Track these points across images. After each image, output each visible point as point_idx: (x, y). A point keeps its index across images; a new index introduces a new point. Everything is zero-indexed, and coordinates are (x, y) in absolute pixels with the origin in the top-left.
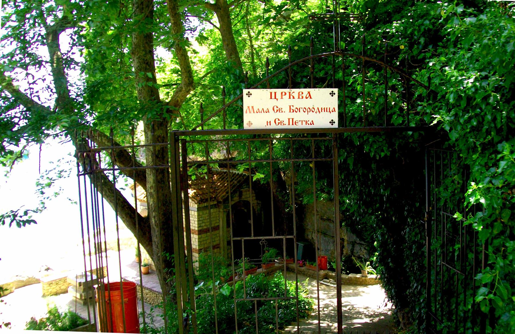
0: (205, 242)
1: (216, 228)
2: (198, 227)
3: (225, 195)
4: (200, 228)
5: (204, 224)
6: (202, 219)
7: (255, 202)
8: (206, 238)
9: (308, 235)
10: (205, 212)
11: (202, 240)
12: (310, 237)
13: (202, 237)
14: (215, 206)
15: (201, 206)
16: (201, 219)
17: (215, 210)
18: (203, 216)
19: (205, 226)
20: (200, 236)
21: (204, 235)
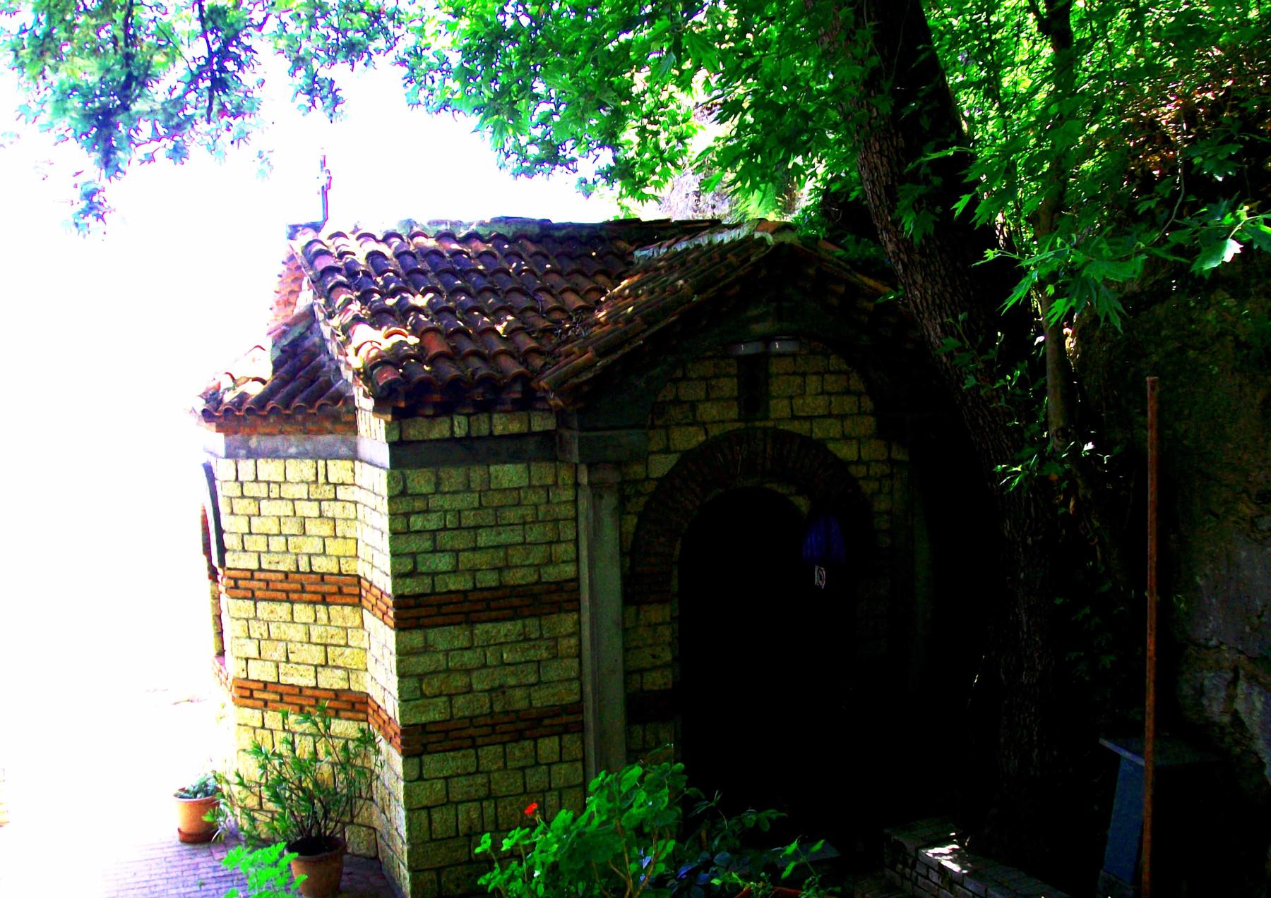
0: (459, 681)
1: (554, 598)
2: (397, 576)
3: (589, 366)
4: (411, 586)
5: (443, 562)
6: (433, 522)
7: (874, 450)
8: (469, 658)
9: (1200, 691)
10: (454, 477)
11: (422, 664)
12: (1215, 709)
13: (427, 649)
14: (547, 447)
15: (417, 430)
16: (417, 522)
17: (544, 472)
18: (435, 502)
19: (455, 571)
20: (416, 638)
21: (441, 638)
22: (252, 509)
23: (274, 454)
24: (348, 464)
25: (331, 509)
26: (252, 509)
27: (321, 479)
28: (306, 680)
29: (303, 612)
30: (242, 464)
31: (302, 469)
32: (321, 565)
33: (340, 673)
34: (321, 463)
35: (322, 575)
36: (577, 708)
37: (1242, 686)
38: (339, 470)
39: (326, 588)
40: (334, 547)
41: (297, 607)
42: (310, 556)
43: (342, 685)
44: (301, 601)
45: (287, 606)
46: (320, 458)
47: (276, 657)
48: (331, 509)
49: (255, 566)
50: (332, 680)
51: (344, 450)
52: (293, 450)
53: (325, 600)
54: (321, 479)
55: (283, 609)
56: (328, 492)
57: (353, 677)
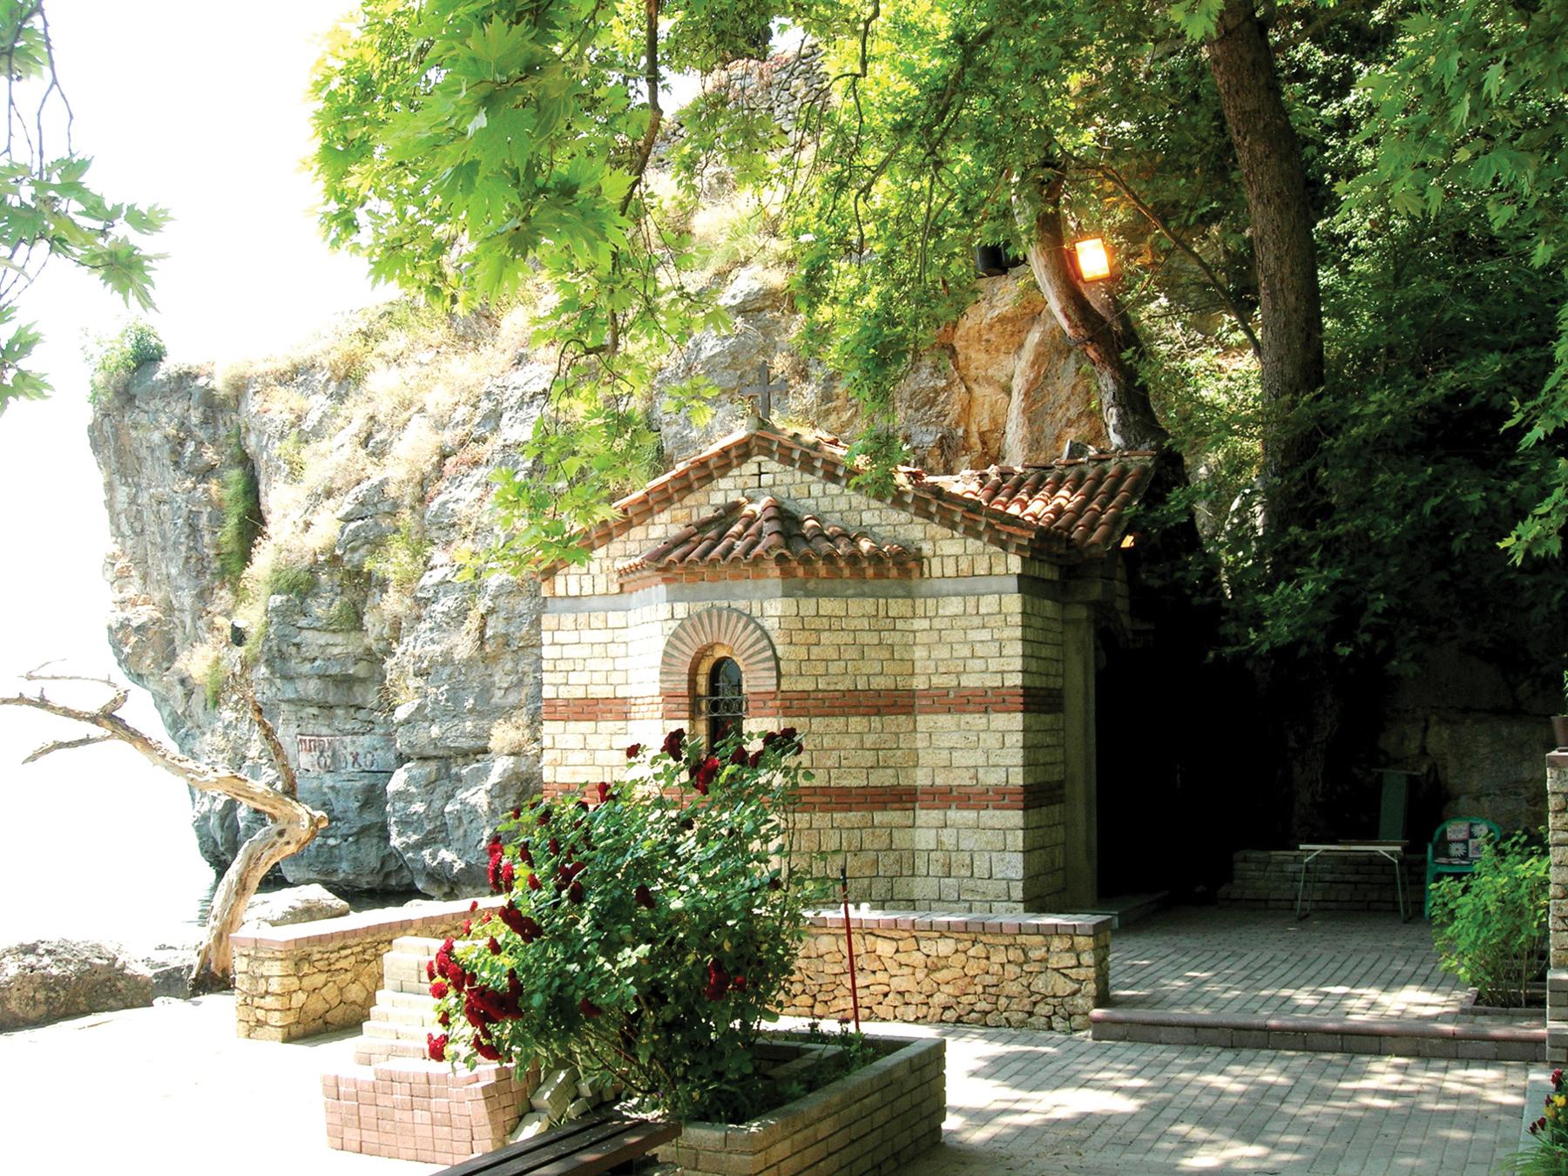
22: (813, 639)
23: (830, 594)
24: (909, 602)
25: (888, 638)
26: (813, 639)
27: (882, 613)
28: (854, 781)
29: (856, 723)
30: (803, 602)
31: (862, 607)
32: (879, 683)
33: (890, 772)
34: (882, 601)
35: (878, 692)
36: (1061, 785)
37: (1433, 730)
38: (897, 607)
39: (881, 702)
40: (890, 667)
41: (853, 720)
42: (868, 676)
43: (893, 781)
44: (857, 714)
45: (842, 719)
46: (878, 597)
47: (829, 763)
48: (888, 638)
49: (810, 686)
50: (883, 778)
51: (900, 592)
52: (850, 592)
53: (878, 711)
54: (882, 613)
55: (838, 723)
56: (888, 623)
57: (902, 774)
